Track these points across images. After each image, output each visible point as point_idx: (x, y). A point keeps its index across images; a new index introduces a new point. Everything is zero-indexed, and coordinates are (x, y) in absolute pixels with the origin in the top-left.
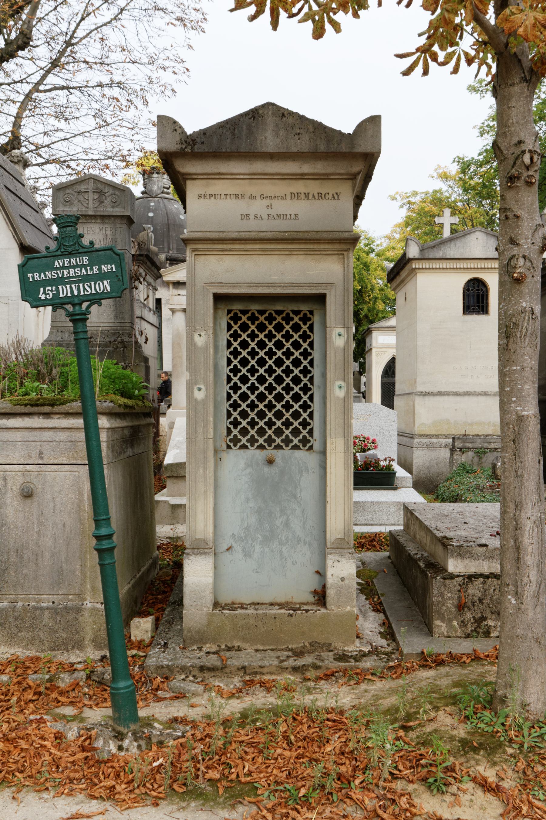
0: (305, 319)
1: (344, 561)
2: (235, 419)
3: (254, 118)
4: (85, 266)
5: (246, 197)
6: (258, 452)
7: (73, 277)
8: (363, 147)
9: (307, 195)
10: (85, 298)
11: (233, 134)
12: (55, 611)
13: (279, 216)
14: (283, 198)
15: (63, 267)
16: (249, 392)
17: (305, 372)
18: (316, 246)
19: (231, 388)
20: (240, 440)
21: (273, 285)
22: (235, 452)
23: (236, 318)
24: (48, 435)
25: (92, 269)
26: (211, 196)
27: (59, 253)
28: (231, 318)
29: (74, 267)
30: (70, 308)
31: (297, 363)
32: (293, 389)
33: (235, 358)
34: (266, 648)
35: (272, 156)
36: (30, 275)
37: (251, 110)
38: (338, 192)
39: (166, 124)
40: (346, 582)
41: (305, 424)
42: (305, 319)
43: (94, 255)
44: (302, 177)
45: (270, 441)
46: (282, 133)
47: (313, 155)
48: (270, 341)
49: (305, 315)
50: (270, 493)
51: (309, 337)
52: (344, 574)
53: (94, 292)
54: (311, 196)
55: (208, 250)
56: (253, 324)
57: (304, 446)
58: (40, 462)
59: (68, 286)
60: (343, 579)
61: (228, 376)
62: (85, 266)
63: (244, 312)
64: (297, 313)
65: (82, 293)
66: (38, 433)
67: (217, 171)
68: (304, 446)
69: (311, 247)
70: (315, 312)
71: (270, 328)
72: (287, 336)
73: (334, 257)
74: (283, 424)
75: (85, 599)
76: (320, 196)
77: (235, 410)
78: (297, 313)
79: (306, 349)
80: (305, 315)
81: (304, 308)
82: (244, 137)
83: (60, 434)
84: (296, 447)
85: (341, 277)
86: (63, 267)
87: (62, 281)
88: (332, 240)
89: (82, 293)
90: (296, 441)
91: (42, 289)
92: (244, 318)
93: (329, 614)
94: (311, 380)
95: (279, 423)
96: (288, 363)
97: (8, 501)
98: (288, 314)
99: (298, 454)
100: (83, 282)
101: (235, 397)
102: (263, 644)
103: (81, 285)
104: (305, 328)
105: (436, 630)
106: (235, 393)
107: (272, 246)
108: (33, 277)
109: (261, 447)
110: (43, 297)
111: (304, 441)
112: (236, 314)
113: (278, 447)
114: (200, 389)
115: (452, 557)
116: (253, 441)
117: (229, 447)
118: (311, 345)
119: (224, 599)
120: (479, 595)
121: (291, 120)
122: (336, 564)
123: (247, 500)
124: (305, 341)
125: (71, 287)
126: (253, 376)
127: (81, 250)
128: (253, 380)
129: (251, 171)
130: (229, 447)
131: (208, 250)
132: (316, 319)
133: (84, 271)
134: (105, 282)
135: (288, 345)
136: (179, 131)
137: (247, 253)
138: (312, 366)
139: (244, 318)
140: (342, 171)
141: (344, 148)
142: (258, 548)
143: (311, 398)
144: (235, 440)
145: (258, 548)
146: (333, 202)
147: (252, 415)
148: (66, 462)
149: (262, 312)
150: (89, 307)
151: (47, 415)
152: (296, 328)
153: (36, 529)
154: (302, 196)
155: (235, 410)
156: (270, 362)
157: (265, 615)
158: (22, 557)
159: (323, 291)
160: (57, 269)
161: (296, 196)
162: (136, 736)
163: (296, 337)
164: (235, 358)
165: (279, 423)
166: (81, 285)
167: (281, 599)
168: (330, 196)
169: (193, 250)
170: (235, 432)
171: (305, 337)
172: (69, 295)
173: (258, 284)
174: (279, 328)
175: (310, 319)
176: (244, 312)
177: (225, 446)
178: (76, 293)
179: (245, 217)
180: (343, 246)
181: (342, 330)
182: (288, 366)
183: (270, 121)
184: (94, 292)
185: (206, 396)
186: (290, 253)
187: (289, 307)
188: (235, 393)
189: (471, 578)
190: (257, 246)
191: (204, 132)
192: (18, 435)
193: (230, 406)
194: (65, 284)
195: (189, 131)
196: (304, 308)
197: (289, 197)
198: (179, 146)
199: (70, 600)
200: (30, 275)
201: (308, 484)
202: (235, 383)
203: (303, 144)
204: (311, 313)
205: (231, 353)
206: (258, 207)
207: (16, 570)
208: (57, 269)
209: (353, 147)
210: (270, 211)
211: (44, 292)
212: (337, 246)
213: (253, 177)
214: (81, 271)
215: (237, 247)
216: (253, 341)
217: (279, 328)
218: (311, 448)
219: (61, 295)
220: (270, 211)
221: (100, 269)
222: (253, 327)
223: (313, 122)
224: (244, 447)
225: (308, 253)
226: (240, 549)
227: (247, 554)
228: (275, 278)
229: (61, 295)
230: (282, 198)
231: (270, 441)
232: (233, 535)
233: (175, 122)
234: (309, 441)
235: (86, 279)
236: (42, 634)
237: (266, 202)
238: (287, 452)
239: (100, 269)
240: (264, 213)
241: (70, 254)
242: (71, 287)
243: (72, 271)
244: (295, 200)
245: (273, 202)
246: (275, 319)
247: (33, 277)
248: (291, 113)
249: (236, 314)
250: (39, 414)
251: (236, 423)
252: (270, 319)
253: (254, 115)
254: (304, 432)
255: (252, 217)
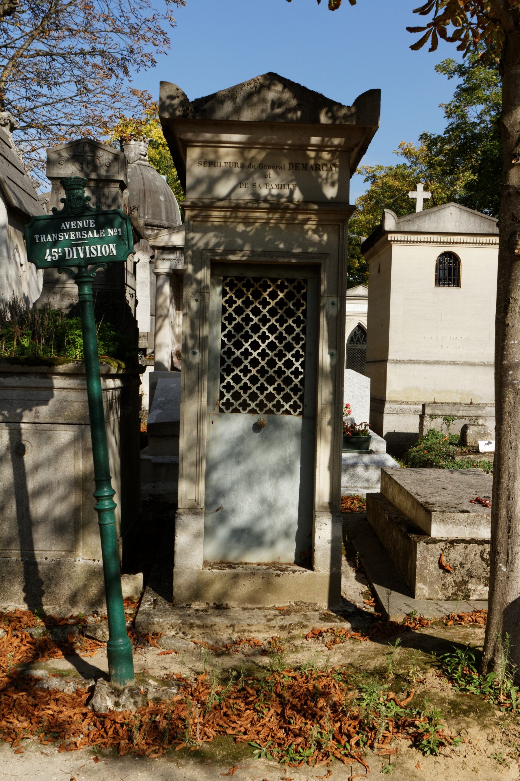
6: (249, 416)
34: (253, 607)
36: (37, 236)
49: (299, 283)
53: (100, 255)
58: (36, 421)
65: (88, 256)
70: (309, 281)
80: (299, 283)
89: (88, 256)
102: (250, 603)
105: (417, 592)
110: (49, 259)
117: (221, 411)
120: (461, 559)
134: (111, 245)
148: (61, 422)
154: (301, 166)
162: (132, 693)
166: (87, 248)
178: (82, 256)
184: (100, 255)
189: (453, 542)
192: (15, 394)
200: (37, 236)
204: (305, 281)
211: (51, 254)
219: (67, 258)
223: (313, 92)
250: (36, 374)
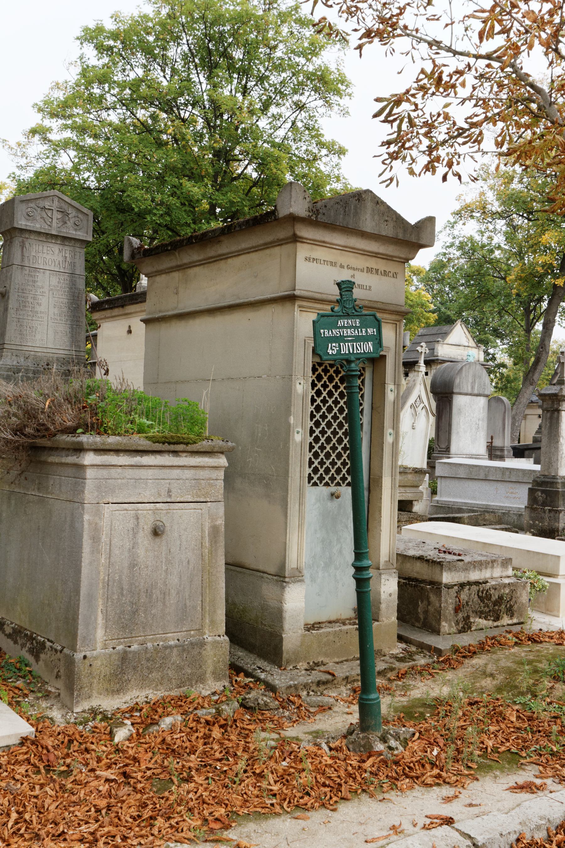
6: (325, 488)
12: (182, 648)
14: (362, 271)
15: (343, 327)
24: (176, 473)
29: (351, 327)
34: (341, 660)
35: (363, 235)
44: (375, 255)
46: (376, 217)
58: (169, 500)
66: (167, 471)
67: (323, 239)
70: (366, 369)
73: (390, 325)
75: (205, 634)
76: (385, 274)
82: (352, 215)
83: (186, 471)
85: (394, 343)
86: (343, 327)
88: (396, 311)
97: (140, 541)
100: (356, 341)
102: (338, 657)
105: (442, 630)
109: (327, 484)
113: (338, 484)
114: (298, 433)
123: (316, 531)
145: (320, 574)
148: (190, 500)
151: (175, 453)
153: (164, 568)
154: (374, 271)
157: (341, 631)
158: (151, 596)
161: (370, 270)
167: (333, 618)
168: (391, 275)
180: (398, 317)
189: (462, 586)
192: (150, 473)
194: (345, 341)
197: (365, 270)
199: (193, 636)
200: (322, 331)
203: (388, 230)
207: (145, 612)
212: (394, 317)
213: (345, 249)
219: (342, 352)
221: (366, 331)
223: (395, 212)
229: (342, 352)
235: (358, 339)
236: (170, 672)
239: (366, 331)
248: (383, 203)
250: (169, 452)
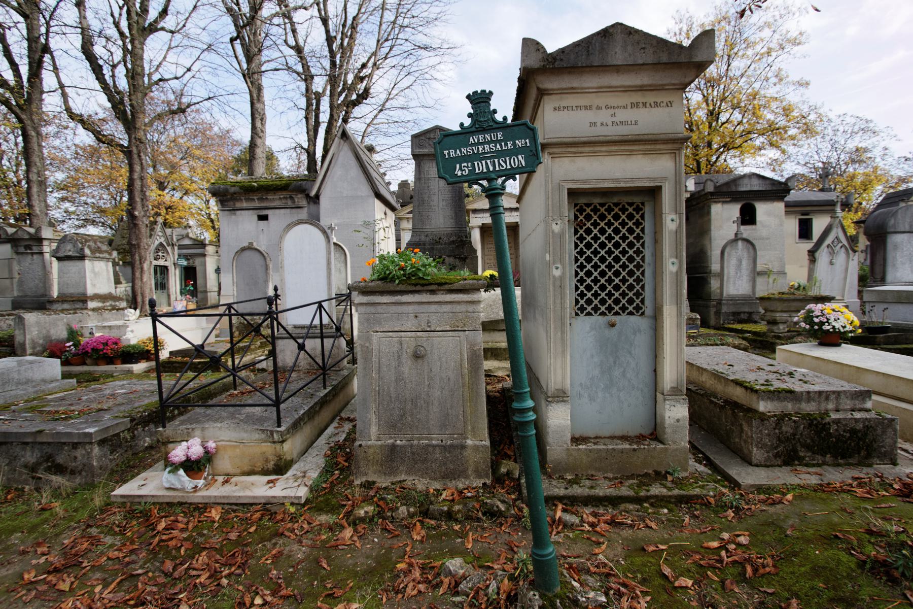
0: (638, 210)
1: (678, 406)
2: (582, 291)
3: (605, 36)
4: (500, 142)
5: (594, 108)
6: (600, 317)
7: (488, 153)
8: (699, 57)
9: (644, 104)
10: (501, 173)
11: (588, 51)
12: (444, 448)
13: (621, 122)
14: (625, 107)
15: (479, 143)
16: (593, 270)
17: (638, 252)
18: (653, 147)
19: (578, 267)
20: (613, 308)
21: (617, 180)
22: (582, 318)
23: (581, 211)
24: (433, 308)
25: (506, 145)
26: (564, 107)
27: (473, 129)
28: (577, 210)
29: (489, 143)
30: (485, 183)
31: (631, 245)
32: (606, 267)
33: (581, 242)
35: (617, 69)
36: (446, 152)
37: (603, 30)
38: (671, 100)
39: (530, 46)
40: (681, 422)
41: (638, 294)
42: (638, 210)
43: (508, 130)
44: (641, 89)
45: (610, 309)
46: (630, 48)
47: (657, 66)
48: (609, 228)
49: (638, 206)
50: (611, 352)
51: (641, 224)
52: (679, 416)
53: (509, 167)
54: (648, 105)
55: (562, 153)
56: (595, 214)
57: (638, 312)
59: (484, 162)
60: (678, 421)
61: (576, 257)
62: (500, 142)
63: (588, 205)
64: (631, 204)
65: (497, 169)
66: (426, 306)
67: (570, 86)
68: (638, 312)
69: (649, 147)
70: (646, 204)
71: (609, 217)
72: (623, 224)
73: (667, 156)
74: (620, 295)
75: (467, 438)
76: (656, 104)
77: (582, 285)
78: (631, 204)
79: (638, 234)
80: (638, 206)
81: (637, 200)
82: (597, 53)
83: (444, 306)
84: (631, 313)
85: (673, 172)
86: (479, 143)
87: (478, 157)
88: (671, 140)
89: (497, 169)
90: (631, 308)
91: (458, 166)
92: (588, 210)
93: (666, 449)
94: (643, 259)
95: (617, 294)
96: (624, 245)
97: (404, 361)
98: (624, 206)
99: (632, 318)
101: (582, 274)
103: (496, 160)
104: (637, 217)
106: (582, 271)
107: (616, 148)
108: (449, 154)
109: (603, 314)
110: (459, 174)
111: (638, 308)
112: (581, 207)
113: (617, 314)
114: (557, 268)
115: (763, 400)
116: (596, 309)
117: (577, 314)
118: (643, 230)
119: (577, 436)
120: (791, 431)
121: (636, 37)
122: (672, 408)
123: (592, 356)
124: (637, 228)
125: (486, 163)
126: (595, 256)
127: (495, 126)
128: (596, 260)
129: (599, 85)
130: (577, 314)
131: (562, 153)
132: (648, 210)
133: (498, 146)
134: (520, 157)
135: (624, 231)
136: (542, 50)
137: (595, 154)
138: (643, 247)
139: (588, 210)
140: (676, 82)
141: (683, 59)
142: (600, 394)
143: (643, 273)
144: (582, 309)
145: (600, 394)
146: (667, 109)
147: (596, 288)
149: (602, 205)
150: (504, 182)
151: (433, 292)
152: (631, 217)
153: (427, 383)
154: (641, 105)
155: (582, 285)
156: (610, 245)
157: (614, 450)
158: (416, 405)
159: (659, 184)
160: (472, 145)
161: (635, 105)
163: (630, 224)
164: (581, 242)
165: (617, 294)
166: (496, 160)
167: (619, 433)
168: (665, 104)
169: (550, 154)
170: (582, 302)
171: (638, 224)
172: (485, 170)
173: (604, 180)
174: (616, 217)
175: (641, 209)
176: (588, 205)
177: (574, 314)
178: (491, 169)
179: (593, 124)
180: (676, 146)
181: (674, 216)
182: (624, 248)
183: (619, 37)
184: (509, 167)
185: (563, 273)
186: (631, 154)
187: (625, 199)
188: (582, 271)
190: (604, 148)
191: (562, 51)
192: (411, 308)
193: (578, 281)
194: (481, 160)
195: (549, 51)
196: (637, 200)
197: (629, 106)
198: (542, 64)
199: (456, 439)
200: (446, 152)
201: (642, 341)
202: (582, 263)
203: (648, 57)
204: (643, 204)
205: (578, 239)
206: (604, 116)
207: (412, 415)
208: (472, 145)
209: (691, 58)
210: (613, 119)
211: (460, 169)
212: (670, 146)
213: (600, 90)
214: (496, 146)
215: (587, 149)
216: (595, 228)
217: (616, 217)
218: (643, 314)
219: (477, 171)
220: (613, 119)
221: (514, 144)
222: (595, 217)
224: (589, 314)
225: (646, 153)
226: (586, 395)
227: (592, 399)
228: (618, 175)
229: (477, 171)
230: (624, 107)
231: (610, 309)
232: (581, 384)
233: (538, 43)
234: (641, 308)
235: (501, 154)
236: (434, 466)
237: (611, 111)
238: (623, 317)
239: (514, 144)
240: (609, 120)
241: (483, 130)
242: (486, 163)
243: (487, 147)
244: (635, 109)
245: (616, 111)
246: (613, 210)
247: (449, 154)
248: (637, 32)
249: (581, 207)
251: (582, 295)
252: (609, 210)
253: (605, 33)
254: (638, 301)
255: (599, 124)
